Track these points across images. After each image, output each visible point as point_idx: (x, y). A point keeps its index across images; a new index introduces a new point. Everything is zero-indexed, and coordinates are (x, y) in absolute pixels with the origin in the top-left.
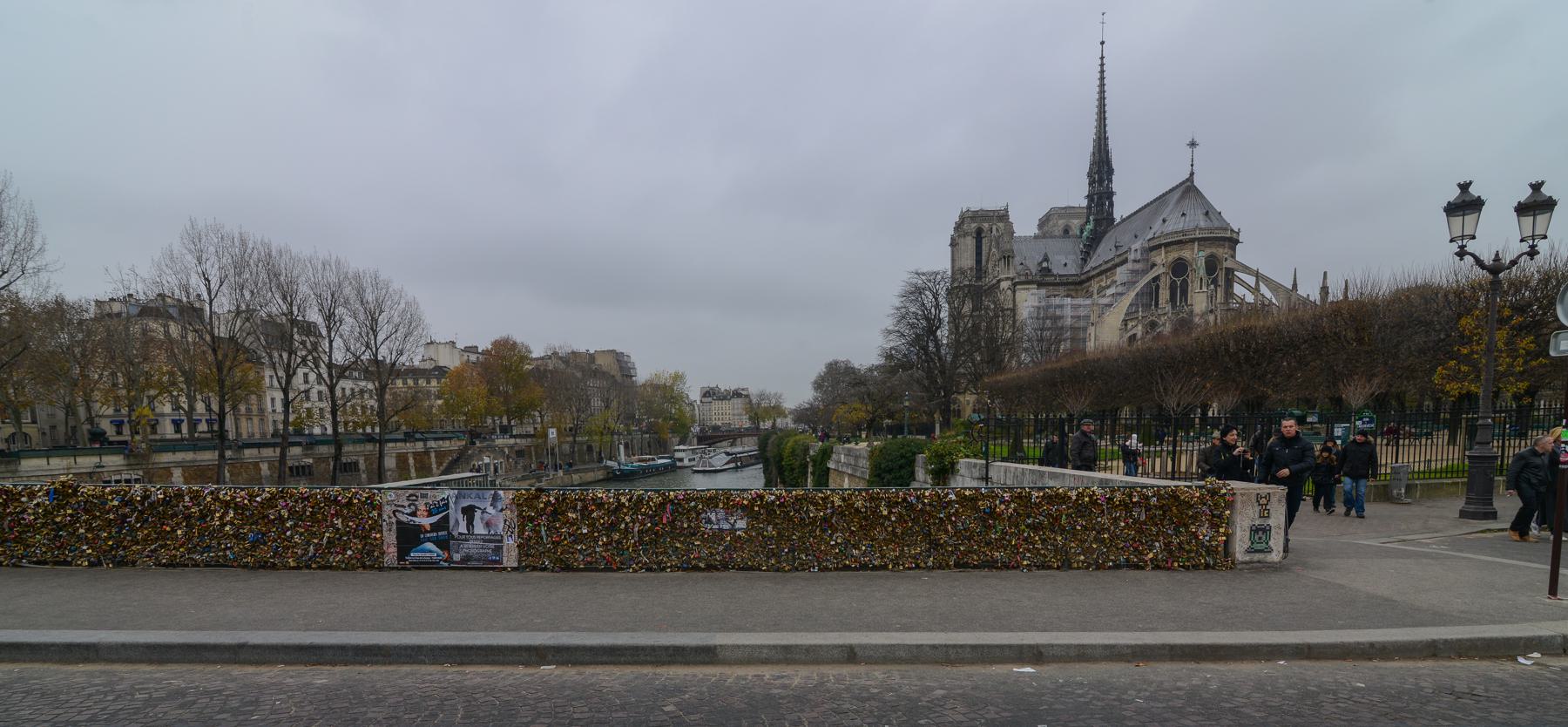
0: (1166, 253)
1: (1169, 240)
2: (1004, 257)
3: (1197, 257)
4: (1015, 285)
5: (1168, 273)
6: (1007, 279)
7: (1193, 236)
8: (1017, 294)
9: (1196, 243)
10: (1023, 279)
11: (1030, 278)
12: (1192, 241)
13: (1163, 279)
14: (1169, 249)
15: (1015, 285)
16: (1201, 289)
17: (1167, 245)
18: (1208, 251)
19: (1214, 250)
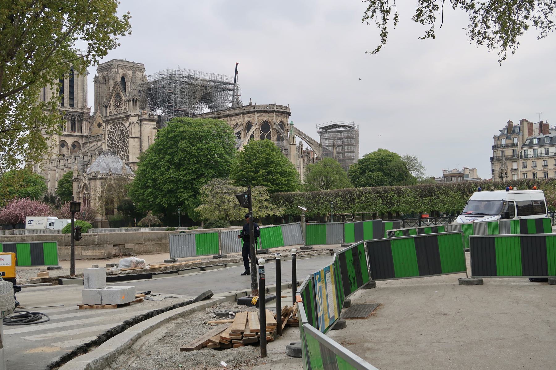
0: (258, 116)
1: (261, 109)
2: (133, 100)
3: (274, 119)
4: (141, 121)
5: (259, 129)
6: (136, 115)
7: (273, 109)
8: (143, 128)
9: (275, 113)
10: (147, 117)
11: (152, 117)
12: (273, 112)
13: (256, 133)
14: (259, 114)
15: (141, 121)
16: (293, 143)
17: (258, 112)
18: (280, 119)
19: (283, 119)
